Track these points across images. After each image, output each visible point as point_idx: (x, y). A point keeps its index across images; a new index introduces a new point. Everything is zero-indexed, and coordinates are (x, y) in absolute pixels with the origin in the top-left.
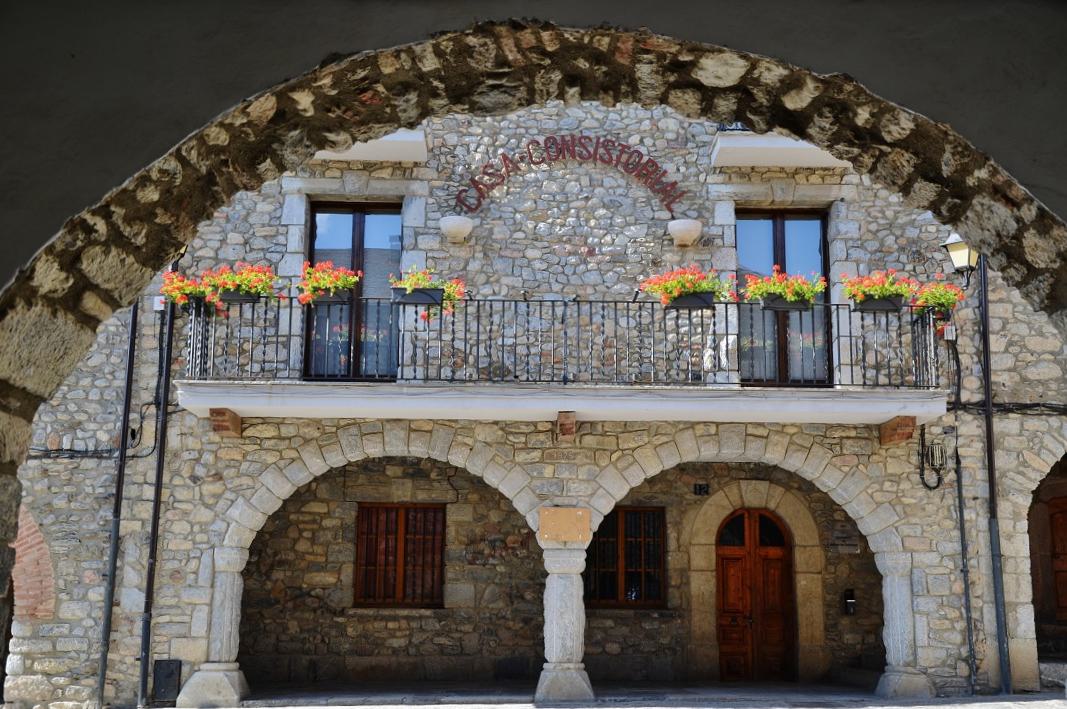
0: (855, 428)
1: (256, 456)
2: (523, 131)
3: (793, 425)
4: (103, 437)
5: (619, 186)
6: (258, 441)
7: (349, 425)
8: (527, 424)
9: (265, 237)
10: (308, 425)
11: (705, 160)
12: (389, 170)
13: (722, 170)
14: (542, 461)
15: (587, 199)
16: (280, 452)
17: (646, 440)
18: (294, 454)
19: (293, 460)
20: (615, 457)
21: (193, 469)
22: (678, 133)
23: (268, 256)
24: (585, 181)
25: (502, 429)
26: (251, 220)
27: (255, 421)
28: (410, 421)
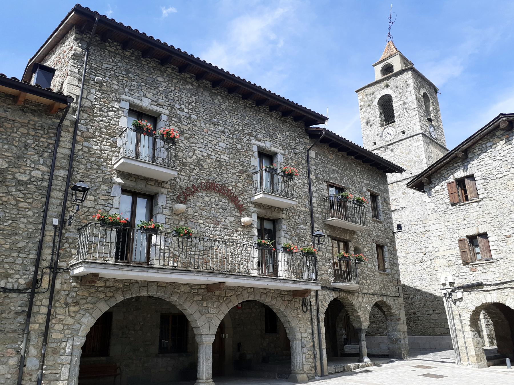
0: (287, 291)
1: (95, 295)
4: (22, 282)
7: (134, 283)
8: (198, 285)
9: (103, 200)
10: (118, 282)
11: (249, 199)
12: (154, 182)
15: (217, 205)
16: (106, 293)
18: (111, 294)
19: (111, 297)
20: (225, 299)
21: (66, 299)
23: (105, 208)
26: (98, 192)
28: (158, 282)
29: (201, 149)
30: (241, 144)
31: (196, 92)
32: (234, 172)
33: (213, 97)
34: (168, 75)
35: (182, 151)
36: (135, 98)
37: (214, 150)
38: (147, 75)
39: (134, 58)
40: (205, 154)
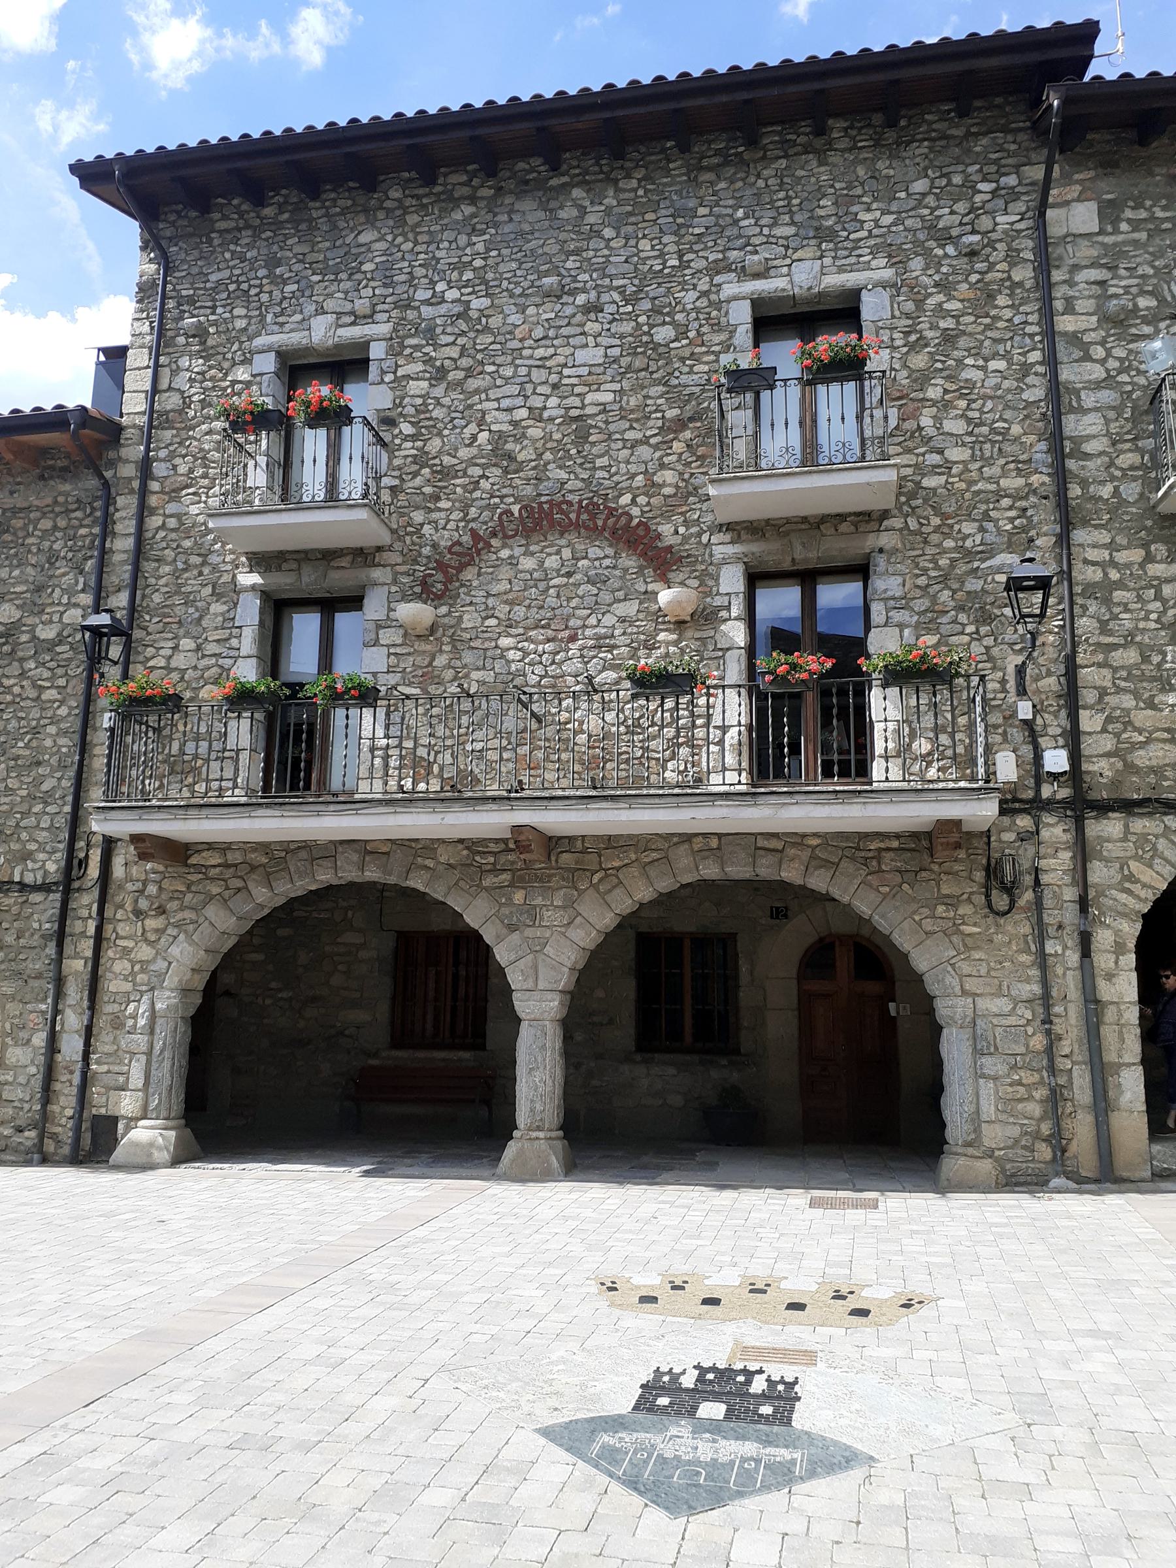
0: (897, 836)
2: (497, 500)
3: (815, 835)
4: (51, 867)
5: (606, 557)
6: (201, 868)
9: (218, 641)
12: (349, 558)
13: (729, 527)
14: (512, 885)
15: (569, 575)
17: (633, 856)
18: (239, 883)
19: (239, 890)
21: (136, 901)
22: (677, 487)
23: (221, 661)
24: (567, 553)
25: (467, 848)
26: (204, 623)
27: (200, 847)
29: (505, 403)
30: (673, 323)
31: (489, 217)
32: (639, 435)
33: (553, 204)
34: (389, 211)
35: (440, 434)
36: (292, 331)
37: (555, 386)
38: (327, 244)
39: (286, 216)
40: (523, 413)
